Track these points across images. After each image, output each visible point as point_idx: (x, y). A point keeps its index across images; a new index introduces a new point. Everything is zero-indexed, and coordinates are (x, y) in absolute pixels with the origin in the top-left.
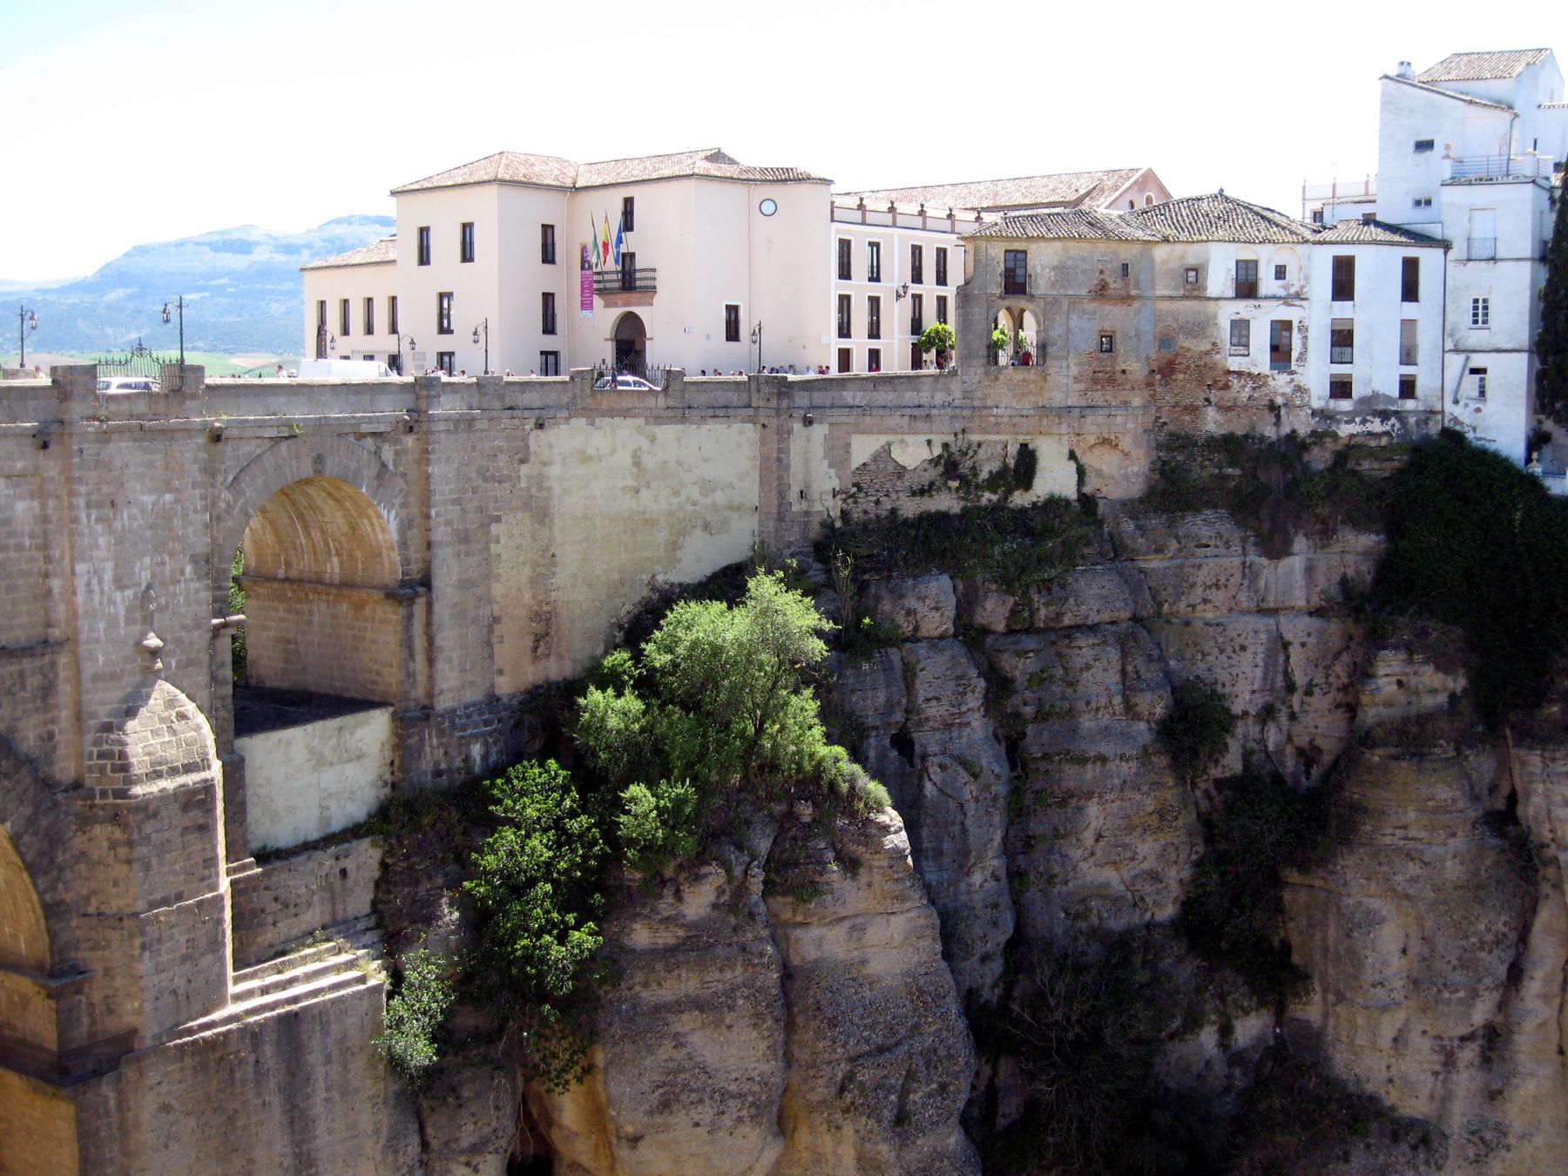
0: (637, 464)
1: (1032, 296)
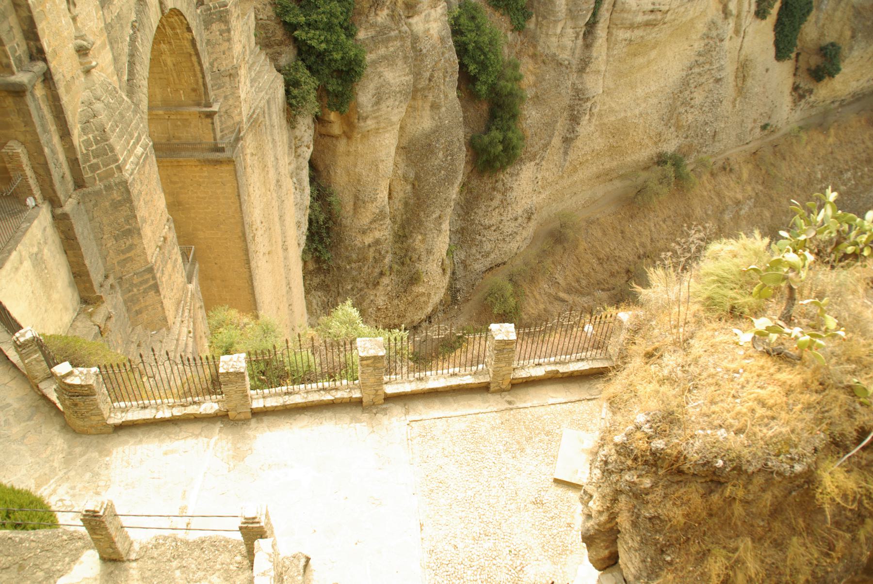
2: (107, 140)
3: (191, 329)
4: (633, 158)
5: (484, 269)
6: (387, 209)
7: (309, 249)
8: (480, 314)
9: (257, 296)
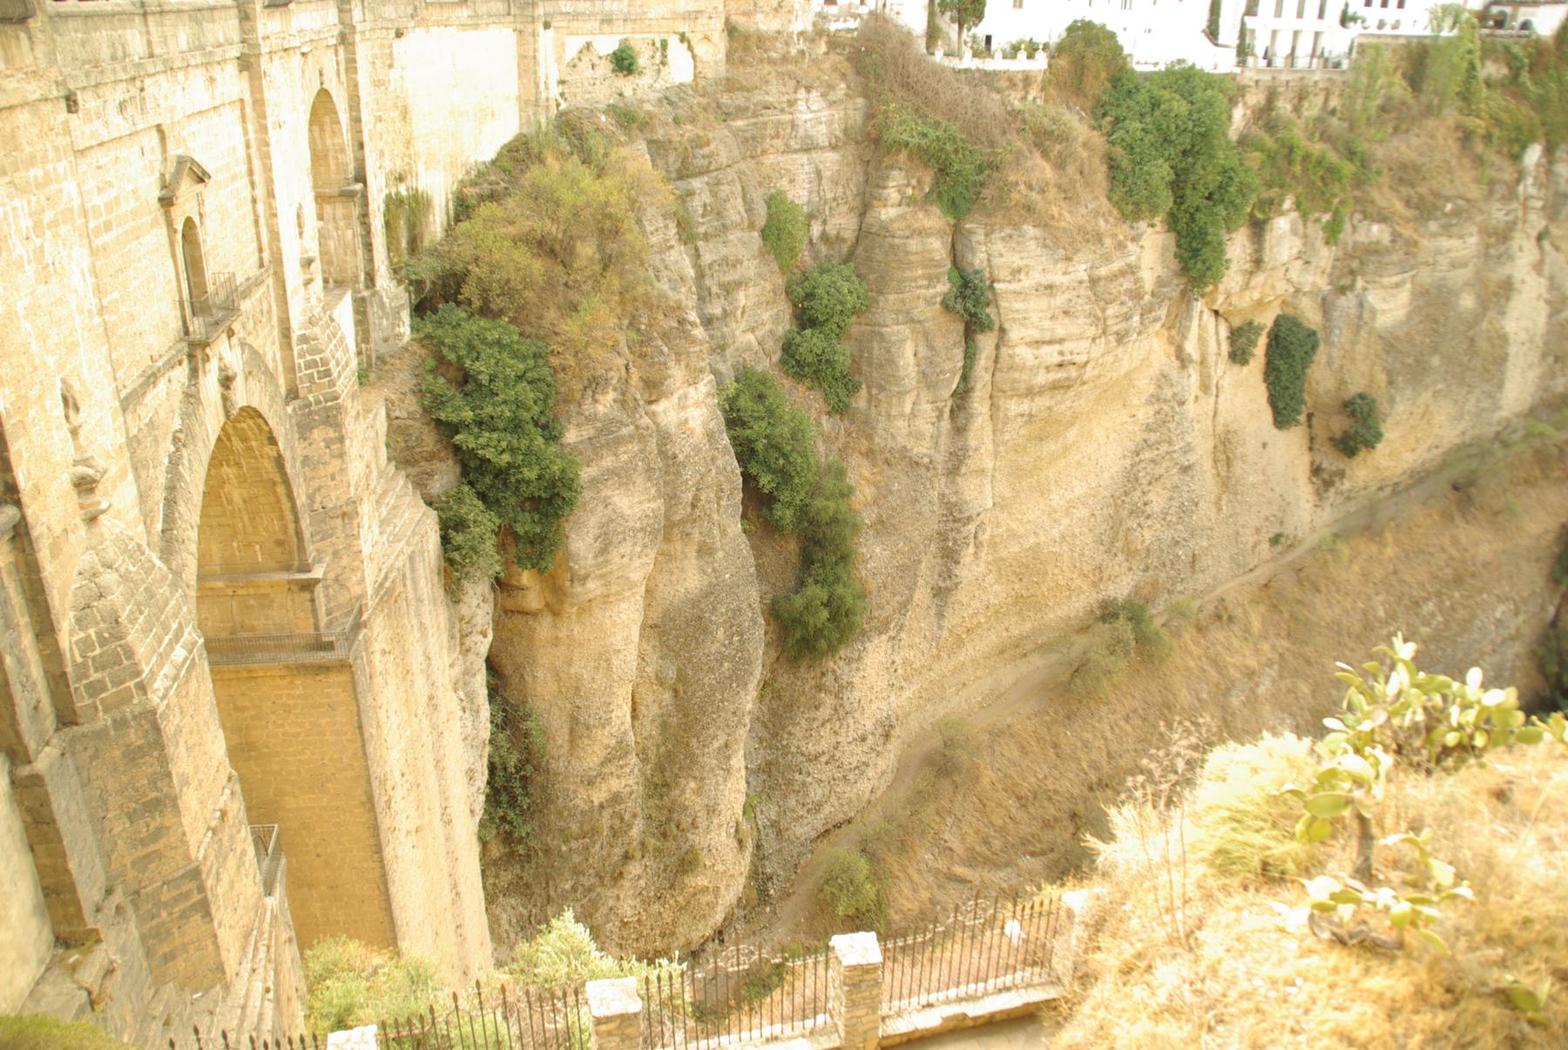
2: (121, 638)
3: (270, 984)
4: (1059, 613)
5: (813, 834)
6: (631, 738)
7: (492, 819)
8: (811, 919)
9: (397, 912)
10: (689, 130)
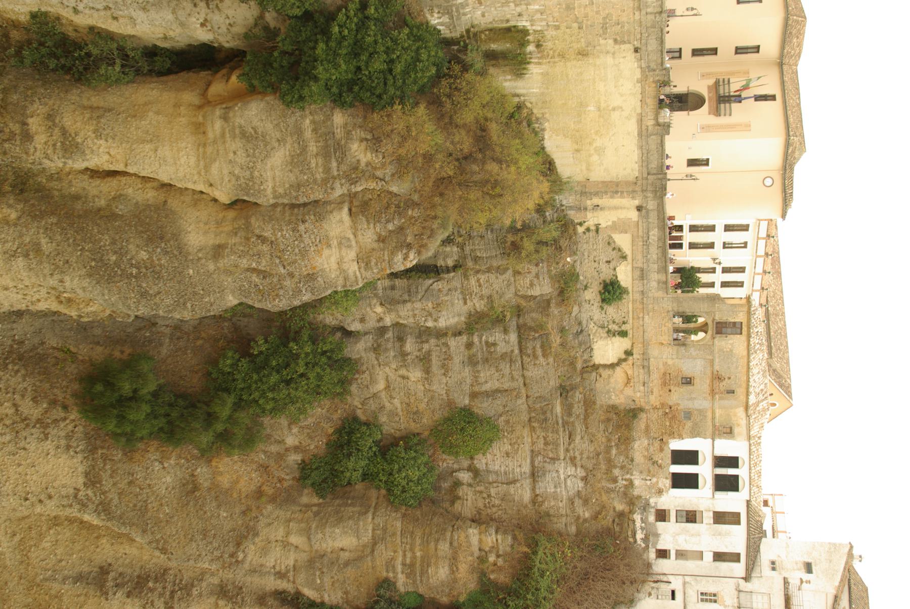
0: (614, 109)
1: (714, 338)
10: (556, 340)
